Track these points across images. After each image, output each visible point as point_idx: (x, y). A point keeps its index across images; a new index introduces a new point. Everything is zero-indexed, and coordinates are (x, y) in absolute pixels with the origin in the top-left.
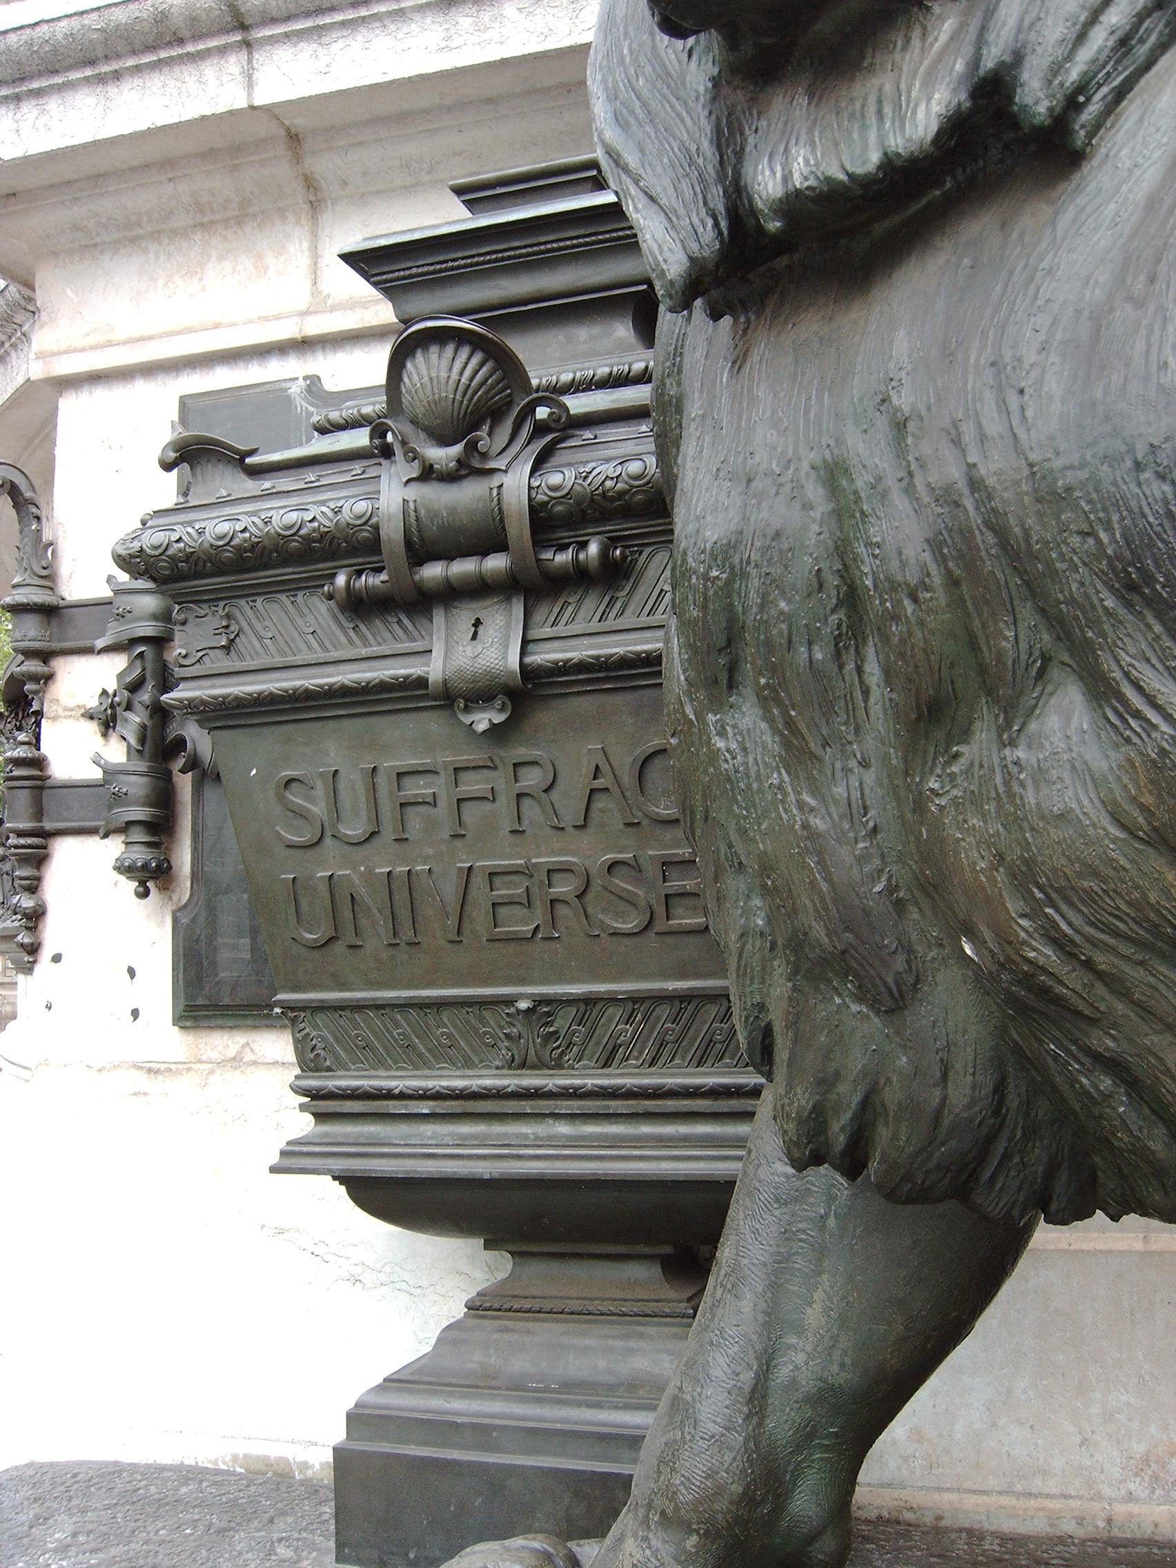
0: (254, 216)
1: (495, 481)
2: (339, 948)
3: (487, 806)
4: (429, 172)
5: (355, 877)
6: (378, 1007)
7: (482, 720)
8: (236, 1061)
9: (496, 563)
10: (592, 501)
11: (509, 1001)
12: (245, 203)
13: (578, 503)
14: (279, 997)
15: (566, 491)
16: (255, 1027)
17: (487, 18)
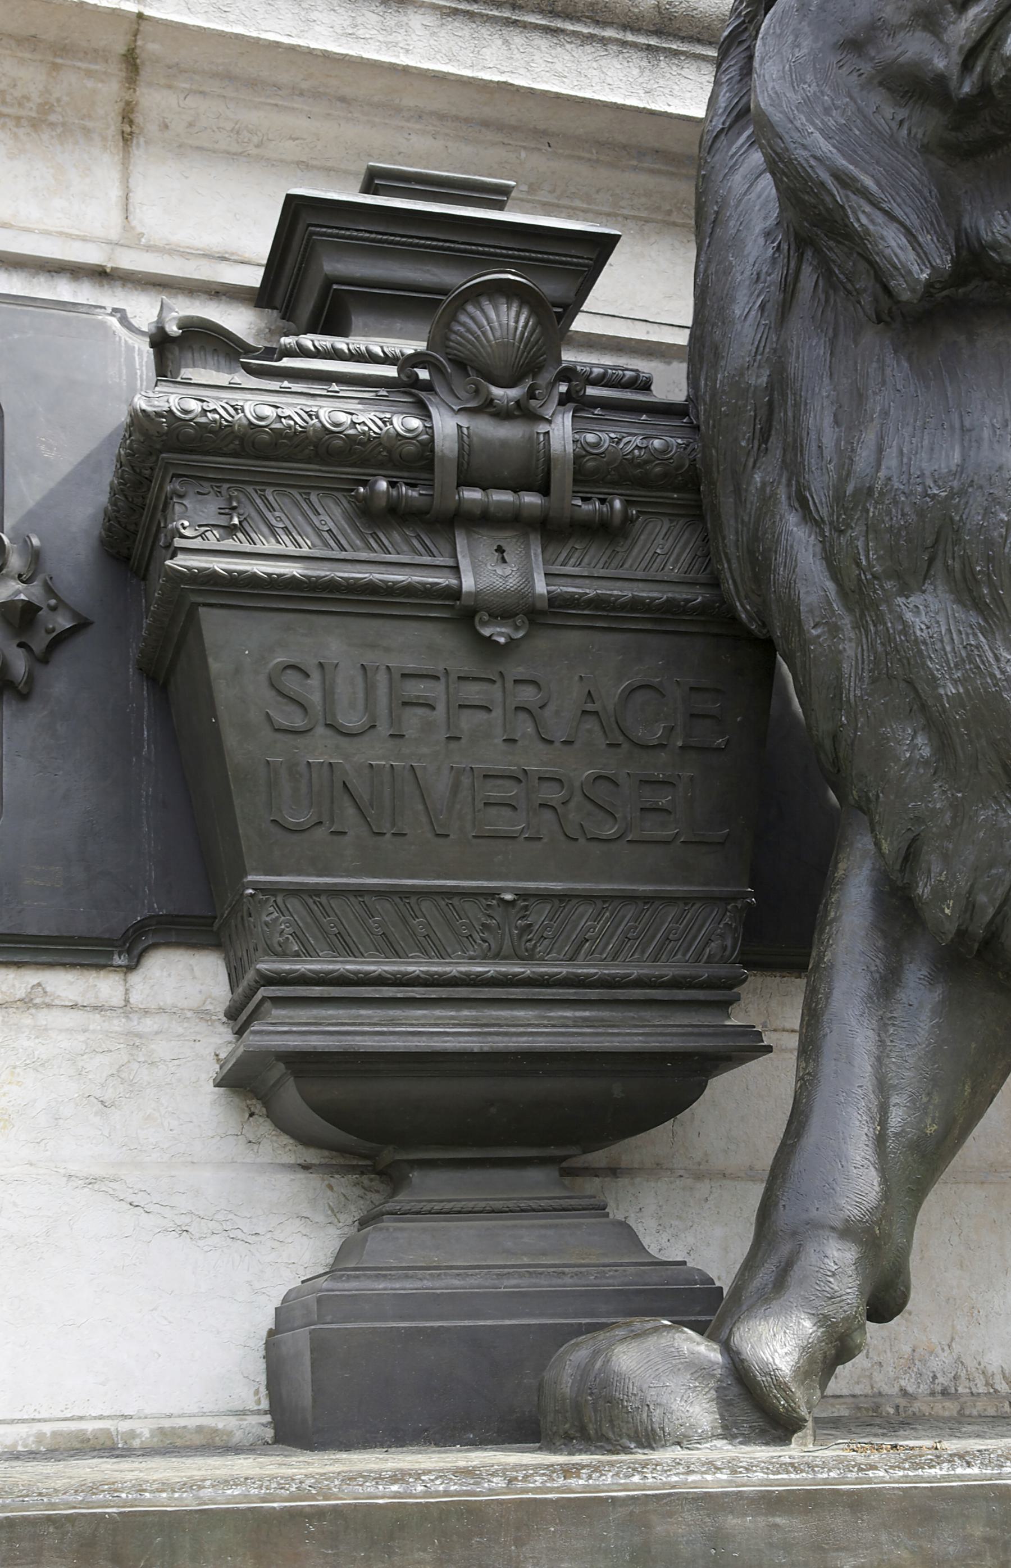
0: (52, 125)
1: (542, 428)
2: (321, 833)
3: (481, 716)
4: (257, 146)
5: (347, 767)
6: (358, 892)
7: (499, 633)
8: (27, 1003)
9: (531, 499)
10: (621, 463)
11: (492, 894)
12: (46, 108)
13: (608, 464)
14: (250, 878)
15: (602, 449)
16: (51, 965)
17: (393, 23)
